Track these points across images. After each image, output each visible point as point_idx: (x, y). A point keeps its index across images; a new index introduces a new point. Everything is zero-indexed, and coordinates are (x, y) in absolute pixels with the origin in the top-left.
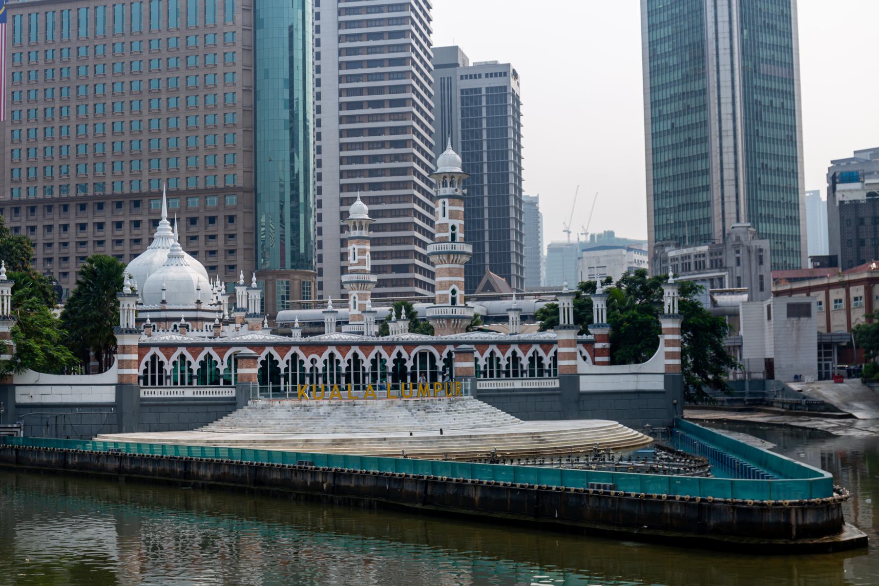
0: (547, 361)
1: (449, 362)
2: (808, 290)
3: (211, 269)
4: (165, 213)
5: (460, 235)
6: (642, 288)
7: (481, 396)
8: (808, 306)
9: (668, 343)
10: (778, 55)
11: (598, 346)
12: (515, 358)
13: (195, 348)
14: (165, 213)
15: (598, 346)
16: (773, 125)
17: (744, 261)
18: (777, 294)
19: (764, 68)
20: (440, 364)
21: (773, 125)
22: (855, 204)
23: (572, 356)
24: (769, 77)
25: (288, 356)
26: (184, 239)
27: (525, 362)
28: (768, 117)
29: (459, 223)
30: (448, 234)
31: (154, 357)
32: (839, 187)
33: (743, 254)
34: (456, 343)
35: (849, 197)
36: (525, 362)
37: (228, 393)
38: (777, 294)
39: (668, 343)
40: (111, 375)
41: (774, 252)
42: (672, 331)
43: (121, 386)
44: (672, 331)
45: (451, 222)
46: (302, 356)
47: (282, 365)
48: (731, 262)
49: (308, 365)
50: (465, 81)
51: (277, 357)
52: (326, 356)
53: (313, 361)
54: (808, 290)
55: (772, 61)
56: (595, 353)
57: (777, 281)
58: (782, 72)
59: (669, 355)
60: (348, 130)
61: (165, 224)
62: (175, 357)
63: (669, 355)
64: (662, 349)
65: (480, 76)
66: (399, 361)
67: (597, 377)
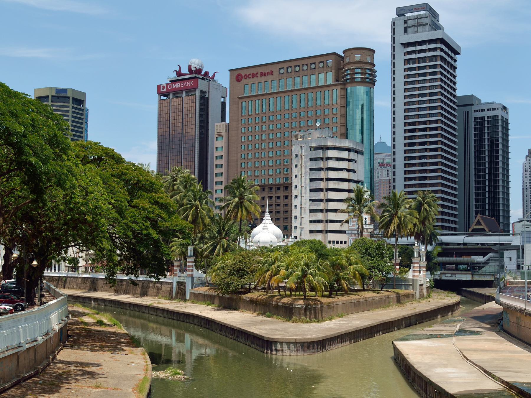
4: (267, 210)
14: (267, 210)
26: (274, 219)
50: (476, 113)
60: (409, 143)
65: (484, 110)
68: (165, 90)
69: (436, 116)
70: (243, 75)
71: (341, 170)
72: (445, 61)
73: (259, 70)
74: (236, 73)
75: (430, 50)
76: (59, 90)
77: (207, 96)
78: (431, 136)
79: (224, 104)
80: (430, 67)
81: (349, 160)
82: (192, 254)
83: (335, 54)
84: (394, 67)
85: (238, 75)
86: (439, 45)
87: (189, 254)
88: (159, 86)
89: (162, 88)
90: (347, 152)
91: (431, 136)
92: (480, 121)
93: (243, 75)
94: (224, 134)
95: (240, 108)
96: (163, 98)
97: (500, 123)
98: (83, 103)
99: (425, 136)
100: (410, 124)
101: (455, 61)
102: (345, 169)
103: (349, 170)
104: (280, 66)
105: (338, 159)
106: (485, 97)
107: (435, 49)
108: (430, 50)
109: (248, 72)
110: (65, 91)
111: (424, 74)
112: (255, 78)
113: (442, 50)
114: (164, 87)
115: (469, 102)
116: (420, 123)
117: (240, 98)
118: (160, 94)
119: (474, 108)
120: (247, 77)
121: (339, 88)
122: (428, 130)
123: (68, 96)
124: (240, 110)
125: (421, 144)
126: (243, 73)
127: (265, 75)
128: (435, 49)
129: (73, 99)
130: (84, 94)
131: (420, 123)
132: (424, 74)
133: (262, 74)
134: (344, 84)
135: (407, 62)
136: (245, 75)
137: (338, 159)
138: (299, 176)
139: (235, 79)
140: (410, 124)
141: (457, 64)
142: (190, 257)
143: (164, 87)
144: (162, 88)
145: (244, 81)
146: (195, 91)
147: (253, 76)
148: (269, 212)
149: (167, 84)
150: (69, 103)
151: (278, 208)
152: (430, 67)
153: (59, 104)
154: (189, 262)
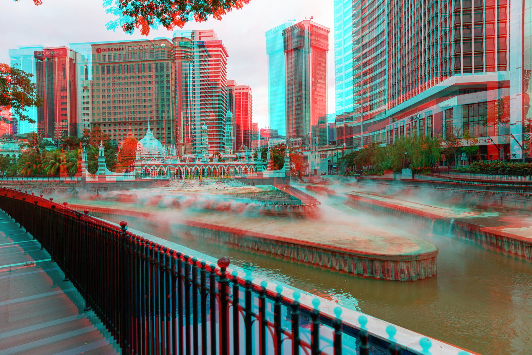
0: (254, 169)
1: (228, 170)
2: (327, 151)
3: (163, 143)
5: (232, 135)
6: (279, 150)
7: (236, 179)
8: (326, 155)
9: (286, 165)
10: (322, 86)
11: (268, 165)
12: (246, 169)
13: (158, 166)
14: (149, 127)
15: (268, 165)
16: (320, 105)
17: (311, 143)
18: (319, 152)
19: (318, 89)
20: (226, 170)
21: (320, 105)
22: (341, 128)
23: (261, 168)
24: (319, 92)
25: (184, 168)
26: (155, 134)
27: (249, 169)
28: (319, 103)
29: (232, 131)
30: (229, 135)
31: (146, 168)
32: (337, 123)
33: (311, 141)
34: (230, 164)
35: (339, 126)
36: (249, 169)
37: (167, 178)
38: (319, 152)
39: (286, 165)
40: (133, 173)
41: (319, 140)
42: (287, 162)
43: (137, 176)
44: (287, 162)
45: (230, 131)
46: (188, 168)
47: (182, 170)
48: (307, 143)
49: (189, 170)
51: (181, 168)
52: (194, 167)
53: (191, 169)
54: (327, 151)
55: (320, 87)
56: (267, 167)
57: (319, 148)
58: (323, 90)
59: (286, 168)
61: (149, 130)
62: (152, 168)
63: (286, 168)
64: (285, 166)
66: (215, 169)
67: (267, 174)
72: (222, 58)
73: (113, 47)
74: (97, 47)
75: (215, 51)
77: (74, 62)
79: (86, 70)
80: (215, 61)
82: (103, 155)
83: (166, 40)
85: (98, 49)
86: (220, 49)
87: (100, 155)
88: (36, 53)
92: (238, 95)
94: (90, 88)
96: (39, 61)
97: (249, 96)
104: (129, 45)
106: (239, 83)
107: (217, 51)
108: (215, 51)
109: (105, 47)
112: (111, 52)
113: (221, 52)
115: (232, 84)
117: (100, 64)
118: (36, 56)
119: (235, 88)
120: (104, 50)
121: (170, 62)
125: (210, 104)
126: (102, 47)
127: (118, 50)
128: (217, 51)
133: (115, 50)
134: (174, 60)
135: (201, 56)
139: (96, 51)
141: (227, 62)
142: (102, 157)
145: (102, 53)
147: (109, 50)
148: (151, 129)
149: (42, 51)
151: (141, 132)
152: (215, 61)
154: (102, 162)
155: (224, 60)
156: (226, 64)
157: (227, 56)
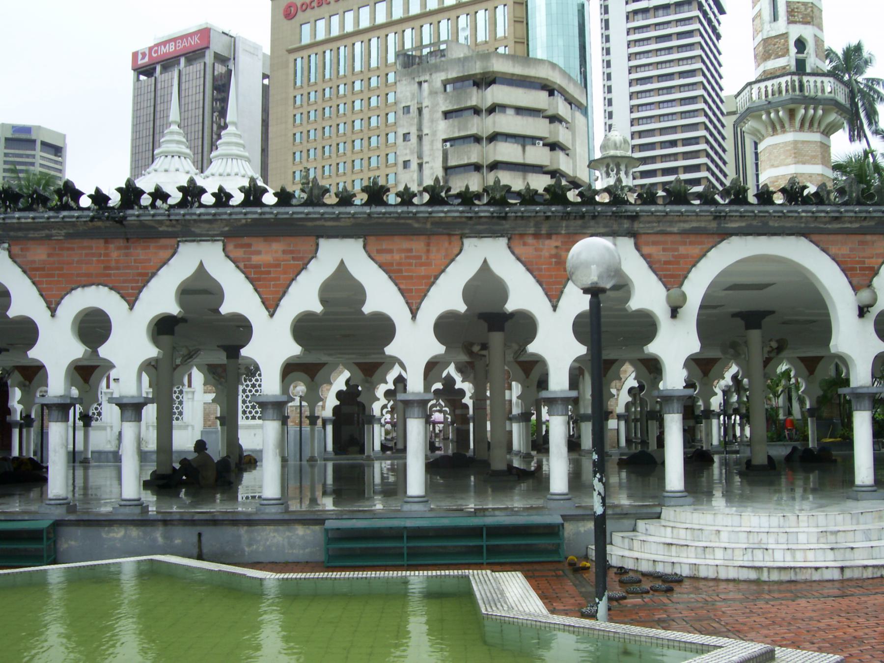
68: (146, 60)
69: (694, 117)
70: (299, 6)
71: (533, 140)
76: (17, 129)
78: (686, 155)
81: (554, 119)
84: (607, 27)
88: (135, 55)
89: (140, 56)
90: (545, 94)
91: (686, 155)
93: (299, 6)
95: (292, 71)
98: (61, 152)
99: (675, 156)
100: (641, 134)
101: (719, 23)
102: (541, 139)
103: (554, 146)
105: (520, 110)
110: (27, 130)
111: (668, 37)
114: (144, 55)
116: (663, 131)
117: (291, 51)
122: (659, 173)
123: (33, 137)
124: (292, 77)
129: (44, 144)
130: (64, 137)
131: (663, 131)
132: (668, 37)
136: (303, 4)
137: (520, 110)
138: (414, 165)
139: (282, 16)
140: (641, 134)
141: (721, 30)
143: (144, 55)
144: (140, 56)
145: (301, 16)
146: (203, 56)
150: (35, 150)
153: (17, 152)
155: (710, 22)
156: (718, 37)
157: (722, 11)
